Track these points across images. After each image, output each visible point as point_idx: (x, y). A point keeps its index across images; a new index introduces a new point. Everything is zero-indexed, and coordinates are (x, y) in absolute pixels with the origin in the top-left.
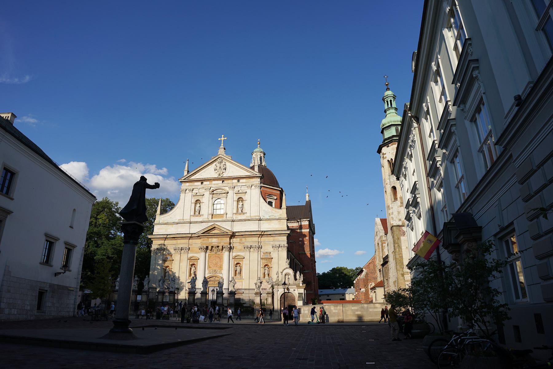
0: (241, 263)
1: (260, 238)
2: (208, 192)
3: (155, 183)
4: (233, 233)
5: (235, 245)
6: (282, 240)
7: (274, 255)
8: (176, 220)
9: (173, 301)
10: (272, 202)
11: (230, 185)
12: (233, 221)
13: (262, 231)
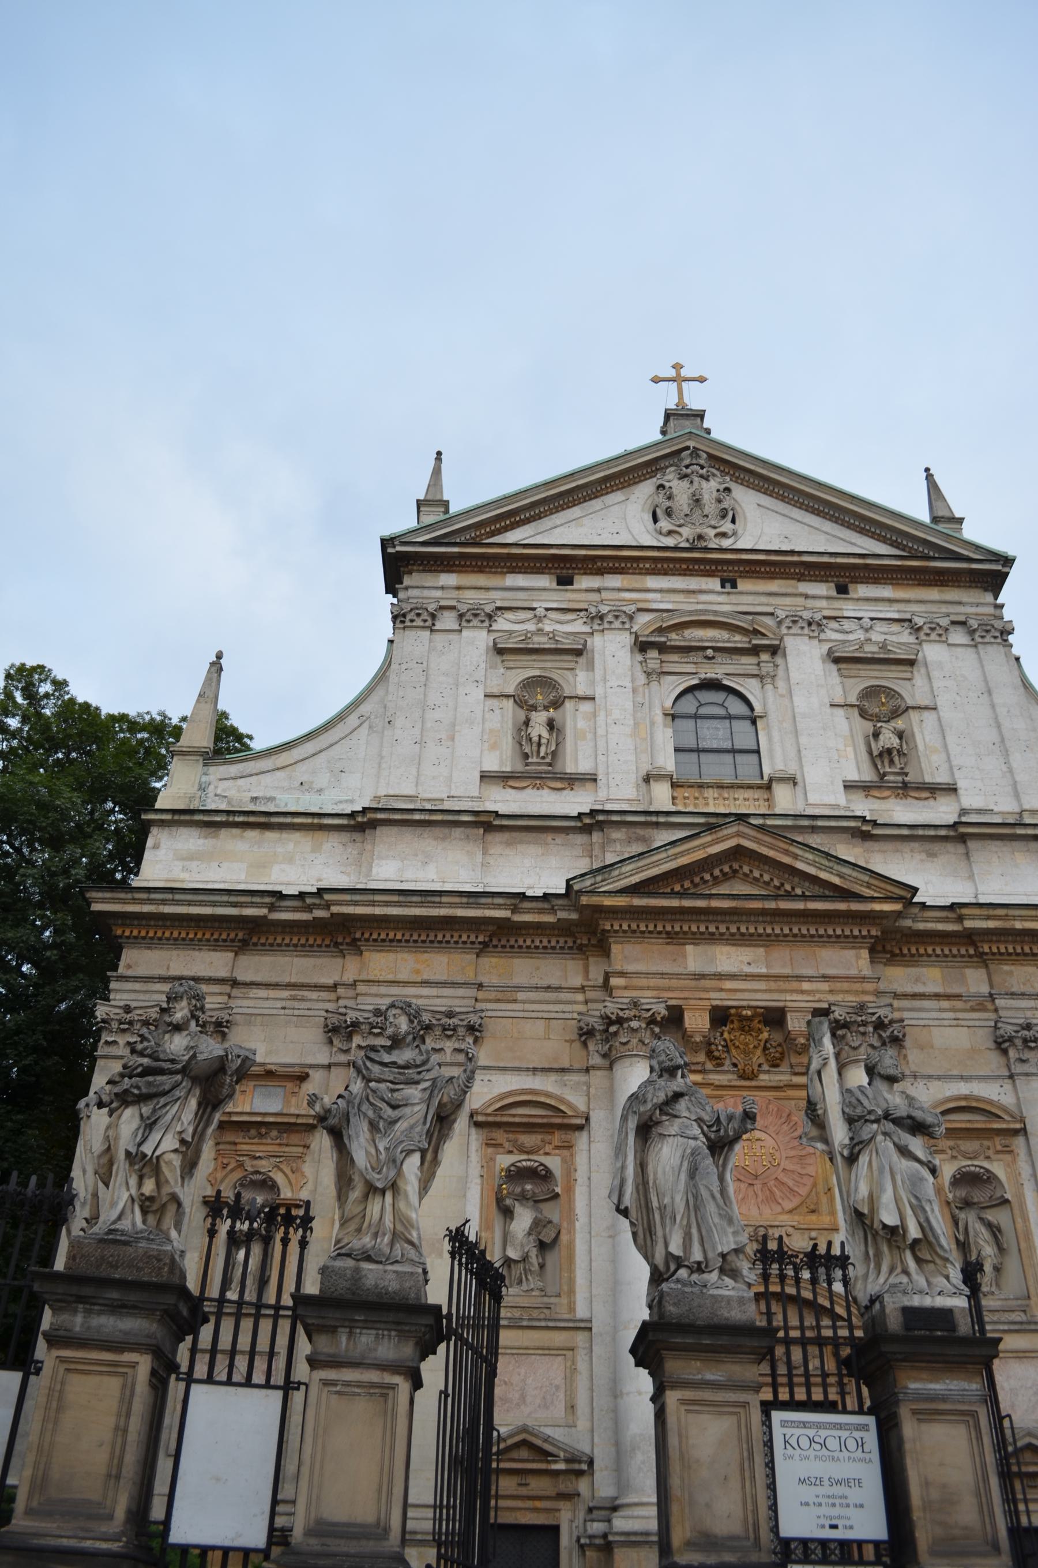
2: (627, 639)
5: (912, 1015)
8: (352, 801)
11: (783, 607)
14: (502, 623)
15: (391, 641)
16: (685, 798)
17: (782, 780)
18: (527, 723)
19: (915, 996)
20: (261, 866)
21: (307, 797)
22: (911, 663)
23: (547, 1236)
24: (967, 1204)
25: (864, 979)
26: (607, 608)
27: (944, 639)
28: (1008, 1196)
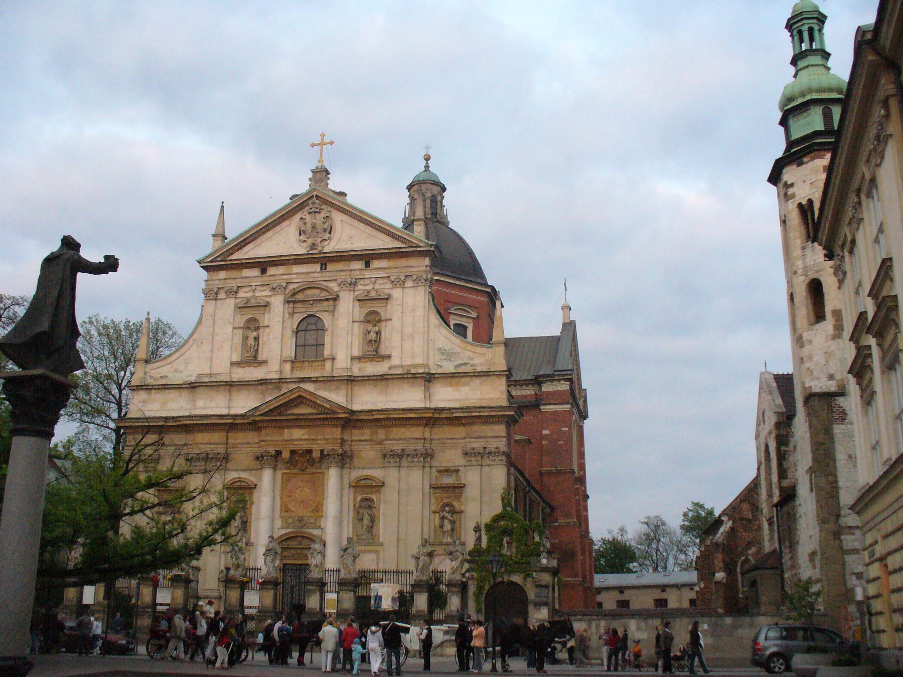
0: (375, 500)
1: (427, 430)
3: (106, 257)
4: (352, 412)
5: (356, 447)
6: (490, 434)
7: (471, 477)
8: (190, 376)
9: (182, 603)
10: (465, 328)
11: (342, 277)
12: (351, 381)
13: (435, 409)
14: (241, 294)
15: (202, 306)
16: (298, 367)
17: (328, 359)
18: (248, 337)
19: (360, 441)
20: (164, 403)
21: (179, 375)
22: (387, 299)
23: (245, 520)
24: (365, 508)
25: (337, 439)
26: (277, 285)
27: (402, 286)
28: (376, 506)
